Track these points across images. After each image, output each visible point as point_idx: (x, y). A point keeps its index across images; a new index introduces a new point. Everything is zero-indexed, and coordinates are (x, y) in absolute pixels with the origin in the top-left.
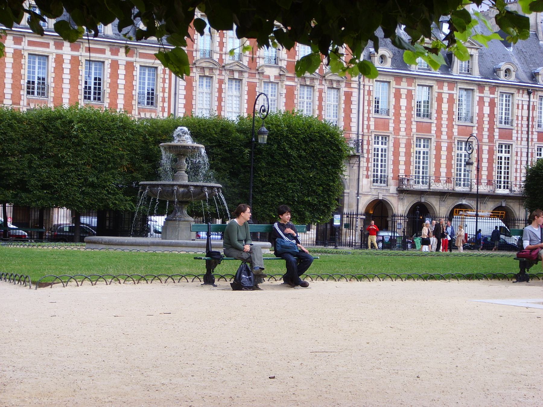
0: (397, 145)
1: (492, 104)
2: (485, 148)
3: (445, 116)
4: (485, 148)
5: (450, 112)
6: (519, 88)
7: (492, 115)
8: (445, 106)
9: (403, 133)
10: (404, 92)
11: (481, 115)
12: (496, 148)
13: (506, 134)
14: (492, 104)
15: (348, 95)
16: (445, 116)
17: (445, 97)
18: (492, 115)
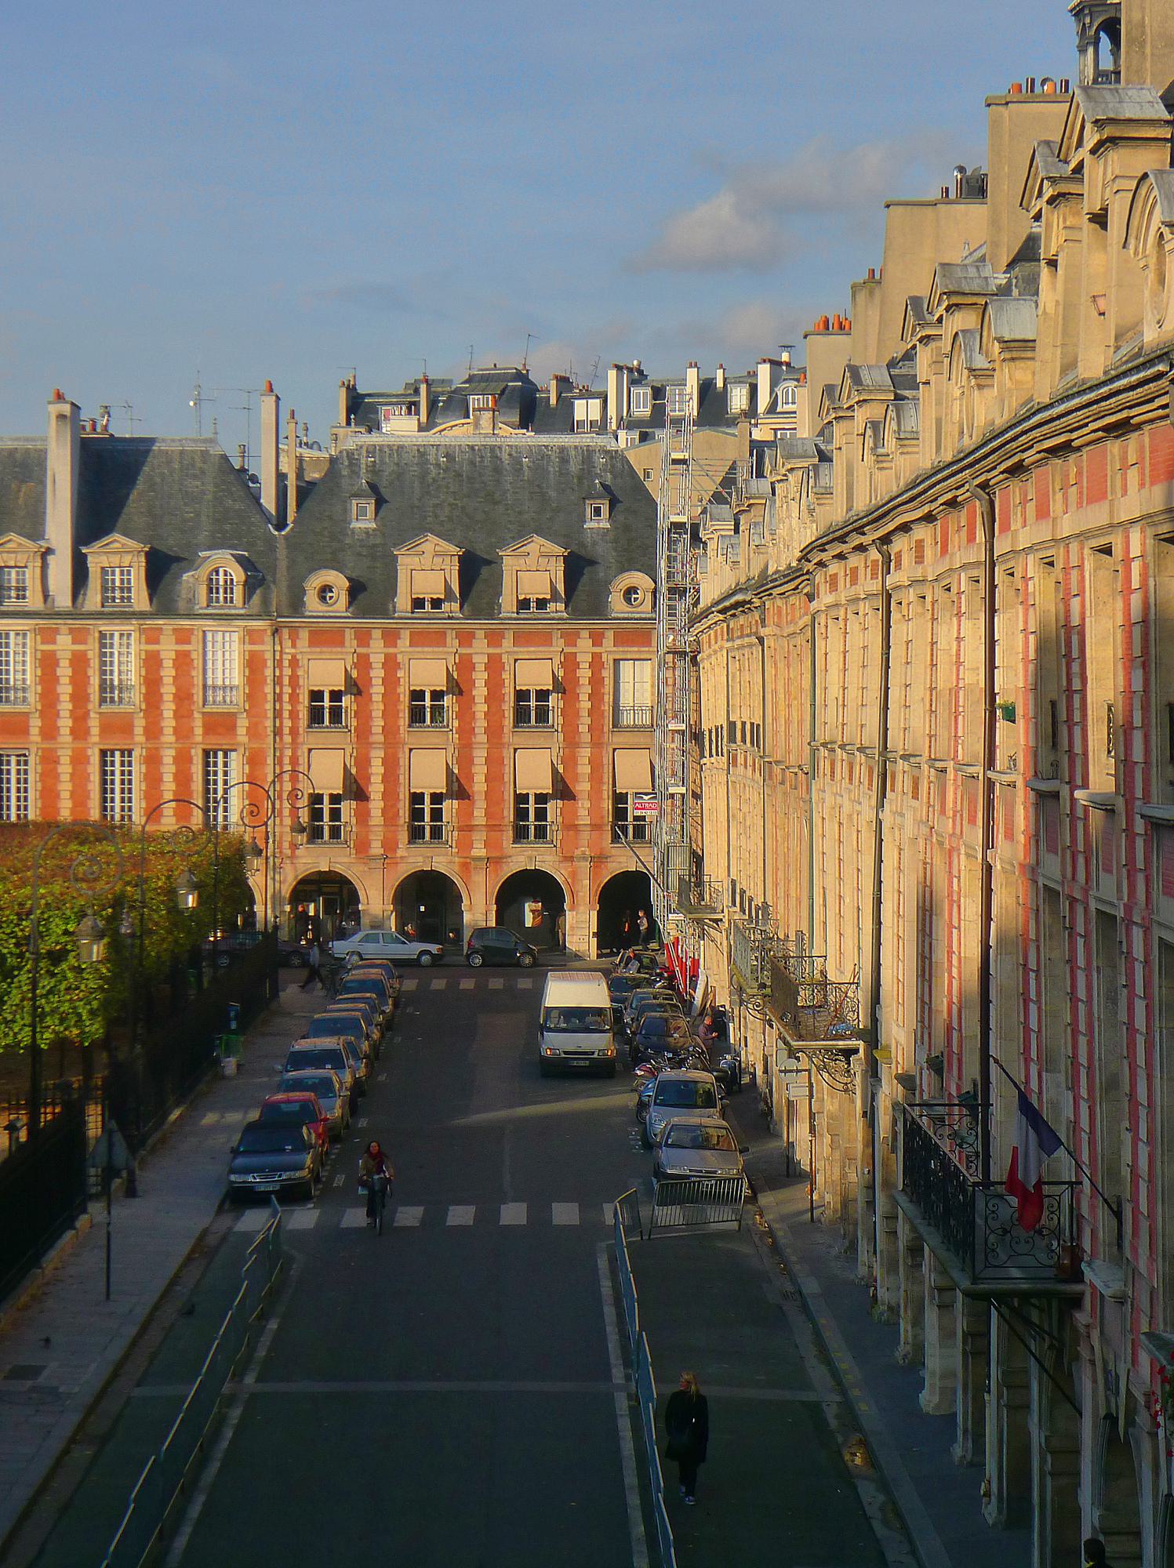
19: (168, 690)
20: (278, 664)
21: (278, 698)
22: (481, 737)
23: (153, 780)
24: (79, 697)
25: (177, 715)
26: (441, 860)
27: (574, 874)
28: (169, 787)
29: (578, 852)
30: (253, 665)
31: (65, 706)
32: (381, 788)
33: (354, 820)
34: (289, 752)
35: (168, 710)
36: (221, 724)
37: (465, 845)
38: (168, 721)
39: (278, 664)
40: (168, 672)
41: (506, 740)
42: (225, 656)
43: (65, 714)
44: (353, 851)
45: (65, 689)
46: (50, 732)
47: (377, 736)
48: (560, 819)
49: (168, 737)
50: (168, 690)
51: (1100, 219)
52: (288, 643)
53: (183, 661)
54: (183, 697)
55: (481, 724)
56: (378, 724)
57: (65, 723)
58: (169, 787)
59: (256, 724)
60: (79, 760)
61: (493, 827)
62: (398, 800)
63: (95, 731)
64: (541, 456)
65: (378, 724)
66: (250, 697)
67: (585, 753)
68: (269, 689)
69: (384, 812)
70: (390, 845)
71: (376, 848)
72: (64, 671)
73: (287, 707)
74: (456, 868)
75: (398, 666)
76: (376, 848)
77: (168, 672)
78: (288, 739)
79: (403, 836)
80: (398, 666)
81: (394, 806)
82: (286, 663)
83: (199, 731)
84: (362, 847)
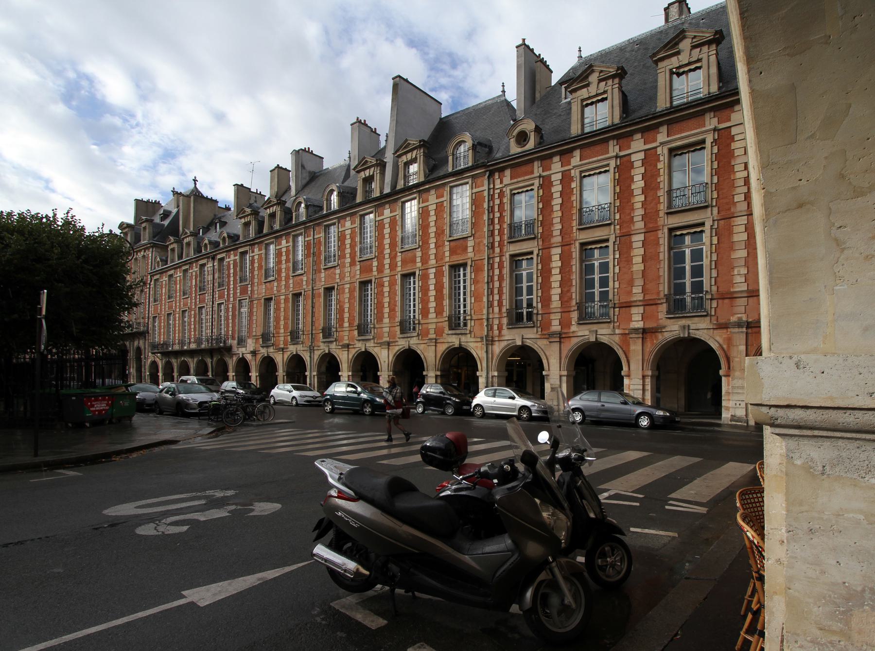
20: (491, 198)
21: (491, 222)
24: (393, 245)
25: (437, 247)
26: (605, 334)
27: (729, 340)
29: (734, 319)
30: (476, 202)
32: (559, 277)
33: (540, 305)
34: (497, 260)
36: (458, 245)
38: (433, 251)
39: (491, 198)
41: (661, 222)
42: (462, 200)
43: (387, 256)
44: (540, 330)
48: (714, 288)
49: (433, 262)
50: (432, 230)
52: (498, 181)
53: (439, 207)
54: (439, 233)
55: (639, 212)
59: (479, 244)
62: (571, 285)
63: (399, 264)
66: (474, 225)
68: (486, 217)
69: (561, 296)
70: (565, 323)
71: (556, 327)
73: (497, 227)
74: (617, 338)
75: (571, 179)
76: (556, 327)
78: (497, 250)
79: (575, 315)
80: (571, 179)
81: (569, 291)
82: (496, 196)
83: (447, 254)
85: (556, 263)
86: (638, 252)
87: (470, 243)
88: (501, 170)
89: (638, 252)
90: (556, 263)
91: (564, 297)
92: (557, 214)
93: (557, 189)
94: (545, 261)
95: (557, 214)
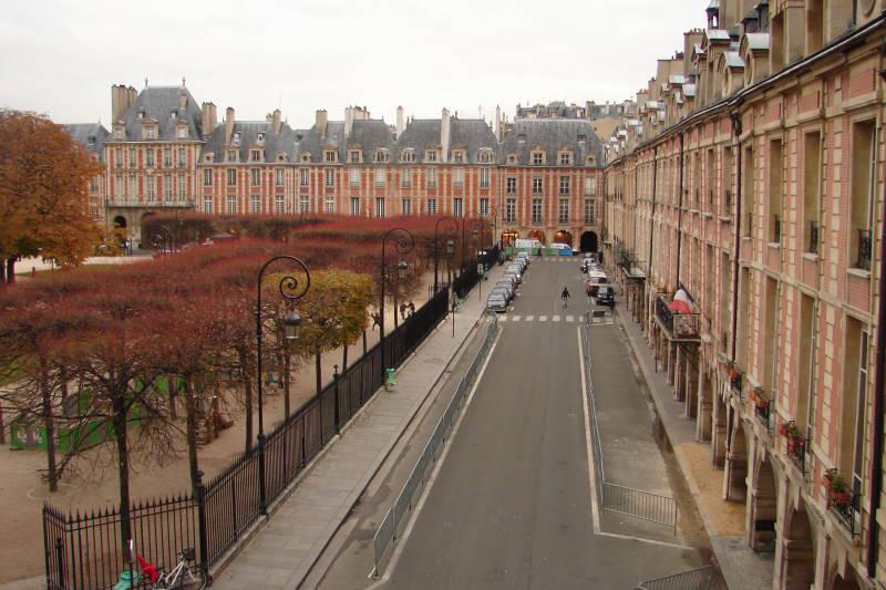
0: (216, 200)
1: (271, 175)
2: (267, 198)
3: (243, 184)
4: (267, 198)
5: (247, 181)
6: (287, 166)
7: (271, 181)
8: (243, 179)
9: (220, 194)
10: (220, 174)
11: (264, 181)
12: (274, 197)
13: (280, 190)
14: (271, 175)
15: (189, 178)
16: (243, 184)
17: (243, 174)
18: (271, 181)
19: (471, 183)
22: (551, 197)
23: (467, 206)
28: (471, 208)
31: (445, 187)
35: (471, 188)
37: (546, 224)
40: (471, 179)
45: (445, 183)
46: (441, 193)
47: (524, 196)
50: (471, 183)
51: (711, 65)
56: (525, 192)
57: (445, 191)
58: (471, 208)
60: (449, 201)
61: (554, 220)
64: (568, 124)
65: (525, 192)
67: (578, 201)
70: (527, 224)
72: (445, 178)
77: (471, 179)
84: (520, 224)
85: (524, 204)
86: (550, 205)
87: (490, 192)
88: (503, 168)
89: (550, 205)
90: (524, 204)
91: (527, 215)
92: (525, 188)
93: (525, 180)
94: (521, 203)
95: (525, 188)
